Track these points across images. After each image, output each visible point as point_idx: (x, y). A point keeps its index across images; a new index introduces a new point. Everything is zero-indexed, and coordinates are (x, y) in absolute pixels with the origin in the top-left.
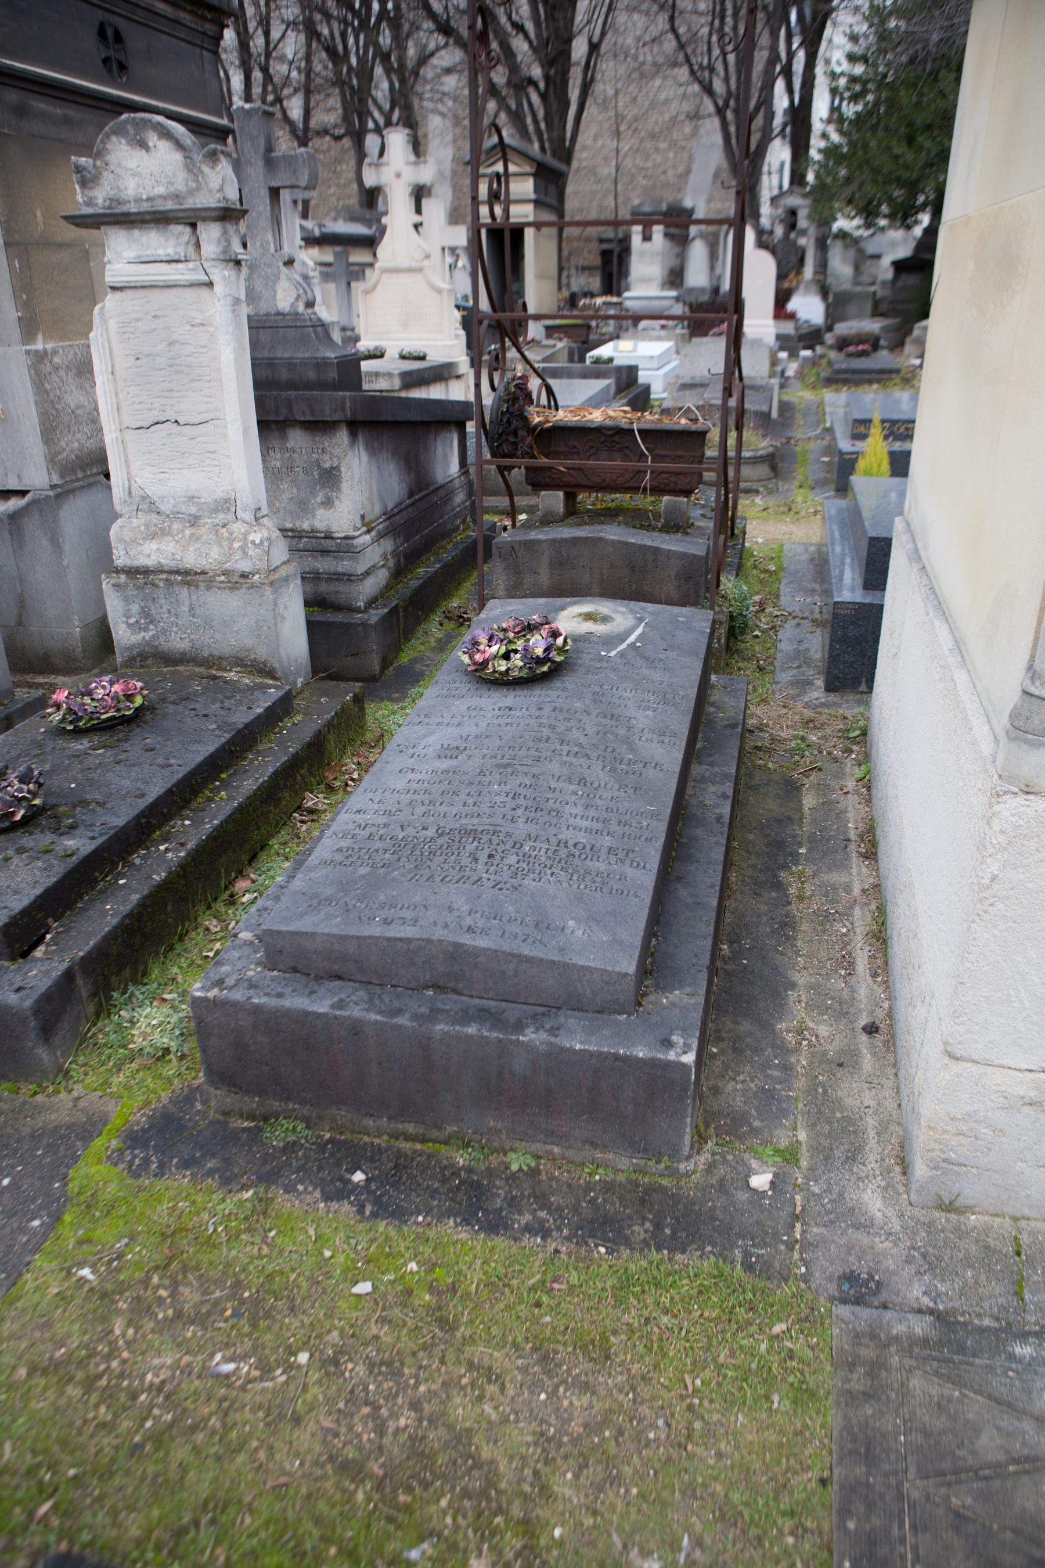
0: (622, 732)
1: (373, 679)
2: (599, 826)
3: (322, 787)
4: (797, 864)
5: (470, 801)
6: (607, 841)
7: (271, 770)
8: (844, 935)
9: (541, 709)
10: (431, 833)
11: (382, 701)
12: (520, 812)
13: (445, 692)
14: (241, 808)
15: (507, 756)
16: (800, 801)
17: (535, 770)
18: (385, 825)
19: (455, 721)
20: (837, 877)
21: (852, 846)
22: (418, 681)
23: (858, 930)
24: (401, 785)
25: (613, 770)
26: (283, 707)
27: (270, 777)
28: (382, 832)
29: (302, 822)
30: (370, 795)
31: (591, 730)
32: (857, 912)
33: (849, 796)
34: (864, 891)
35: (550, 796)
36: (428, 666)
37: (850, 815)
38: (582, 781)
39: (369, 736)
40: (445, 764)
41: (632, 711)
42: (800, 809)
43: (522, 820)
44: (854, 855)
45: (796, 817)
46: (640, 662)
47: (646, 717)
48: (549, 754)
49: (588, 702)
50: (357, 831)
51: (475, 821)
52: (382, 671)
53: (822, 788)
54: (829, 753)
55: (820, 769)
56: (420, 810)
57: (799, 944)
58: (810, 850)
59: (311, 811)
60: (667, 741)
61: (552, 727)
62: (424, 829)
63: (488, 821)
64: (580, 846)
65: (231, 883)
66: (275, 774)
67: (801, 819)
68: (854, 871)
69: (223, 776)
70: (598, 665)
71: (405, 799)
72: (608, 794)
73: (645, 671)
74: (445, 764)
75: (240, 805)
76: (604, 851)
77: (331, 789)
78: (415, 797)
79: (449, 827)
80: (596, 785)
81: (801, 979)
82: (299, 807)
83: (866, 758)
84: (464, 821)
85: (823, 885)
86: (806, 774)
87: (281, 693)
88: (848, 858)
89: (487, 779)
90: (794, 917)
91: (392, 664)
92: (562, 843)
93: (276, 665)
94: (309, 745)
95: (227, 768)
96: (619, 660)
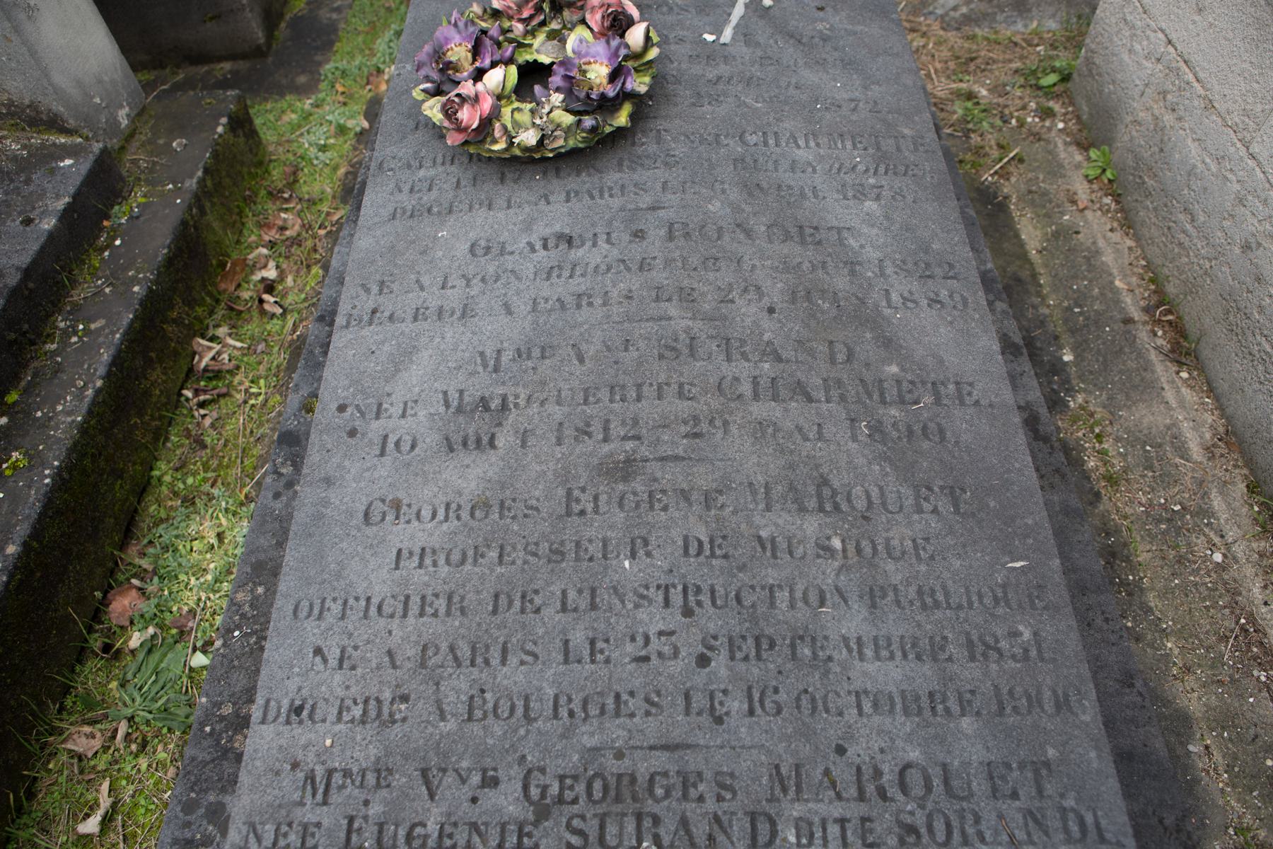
0: (841, 282)
1: (259, 53)
2: (924, 676)
3: (220, 312)
4: (1071, 391)
5: (578, 638)
6: (970, 743)
7: (106, 356)
8: (1220, 567)
9: (639, 235)
10: (507, 802)
11: (282, 95)
12: (720, 663)
13: (406, 200)
14: (62, 482)
15: (617, 430)
16: (1017, 236)
17: (704, 478)
18: (382, 773)
19: (454, 298)
20: (1146, 417)
21: (1143, 334)
22: (331, 44)
23: (1239, 549)
24: (379, 581)
25: (877, 429)
26: (104, 184)
27: (108, 376)
28: (375, 810)
29: (202, 405)
30: (312, 631)
31: (776, 291)
32: (1217, 503)
33: (1088, 214)
34: (1209, 450)
35: (772, 576)
36: (338, 10)
37: (1108, 258)
38: (827, 498)
39: (276, 173)
40: (470, 476)
41: (838, 211)
42: (1024, 257)
43: (736, 705)
44: (1153, 356)
45: (1025, 274)
46: (790, 53)
47: (869, 220)
48: (715, 403)
49: (734, 194)
50: (308, 814)
51: (616, 732)
52: (270, 35)
53: (1038, 200)
54: (1021, 123)
55: (1021, 161)
56: (457, 687)
57: (1152, 600)
58: (1078, 349)
59: (215, 374)
60: (944, 293)
61: (687, 297)
62: (491, 782)
63: (652, 729)
64: (914, 777)
65: (97, 614)
66: (117, 361)
67: (1034, 276)
68: (1169, 395)
69: (12, 397)
70: (711, 74)
71: (405, 634)
72: (900, 533)
73: (810, 76)
74: (470, 476)
75: (58, 474)
76: (979, 786)
77: (235, 316)
78: (431, 628)
79: (556, 766)
80: (861, 504)
81: (1193, 698)
82: (191, 370)
83: (1094, 132)
84: (588, 736)
85: (1136, 439)
86: (1004, 174)
87: (85, 167)
88: (1147, 367)
89: (593, 530)
90: (1117, 531)
91: (281, 16)
92: (868, 784)
93: (59, 108)
94: (170, 262)
95: (14, 379)
96: (743, 50)
